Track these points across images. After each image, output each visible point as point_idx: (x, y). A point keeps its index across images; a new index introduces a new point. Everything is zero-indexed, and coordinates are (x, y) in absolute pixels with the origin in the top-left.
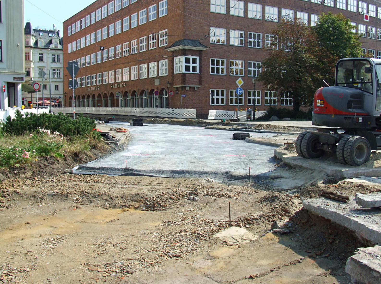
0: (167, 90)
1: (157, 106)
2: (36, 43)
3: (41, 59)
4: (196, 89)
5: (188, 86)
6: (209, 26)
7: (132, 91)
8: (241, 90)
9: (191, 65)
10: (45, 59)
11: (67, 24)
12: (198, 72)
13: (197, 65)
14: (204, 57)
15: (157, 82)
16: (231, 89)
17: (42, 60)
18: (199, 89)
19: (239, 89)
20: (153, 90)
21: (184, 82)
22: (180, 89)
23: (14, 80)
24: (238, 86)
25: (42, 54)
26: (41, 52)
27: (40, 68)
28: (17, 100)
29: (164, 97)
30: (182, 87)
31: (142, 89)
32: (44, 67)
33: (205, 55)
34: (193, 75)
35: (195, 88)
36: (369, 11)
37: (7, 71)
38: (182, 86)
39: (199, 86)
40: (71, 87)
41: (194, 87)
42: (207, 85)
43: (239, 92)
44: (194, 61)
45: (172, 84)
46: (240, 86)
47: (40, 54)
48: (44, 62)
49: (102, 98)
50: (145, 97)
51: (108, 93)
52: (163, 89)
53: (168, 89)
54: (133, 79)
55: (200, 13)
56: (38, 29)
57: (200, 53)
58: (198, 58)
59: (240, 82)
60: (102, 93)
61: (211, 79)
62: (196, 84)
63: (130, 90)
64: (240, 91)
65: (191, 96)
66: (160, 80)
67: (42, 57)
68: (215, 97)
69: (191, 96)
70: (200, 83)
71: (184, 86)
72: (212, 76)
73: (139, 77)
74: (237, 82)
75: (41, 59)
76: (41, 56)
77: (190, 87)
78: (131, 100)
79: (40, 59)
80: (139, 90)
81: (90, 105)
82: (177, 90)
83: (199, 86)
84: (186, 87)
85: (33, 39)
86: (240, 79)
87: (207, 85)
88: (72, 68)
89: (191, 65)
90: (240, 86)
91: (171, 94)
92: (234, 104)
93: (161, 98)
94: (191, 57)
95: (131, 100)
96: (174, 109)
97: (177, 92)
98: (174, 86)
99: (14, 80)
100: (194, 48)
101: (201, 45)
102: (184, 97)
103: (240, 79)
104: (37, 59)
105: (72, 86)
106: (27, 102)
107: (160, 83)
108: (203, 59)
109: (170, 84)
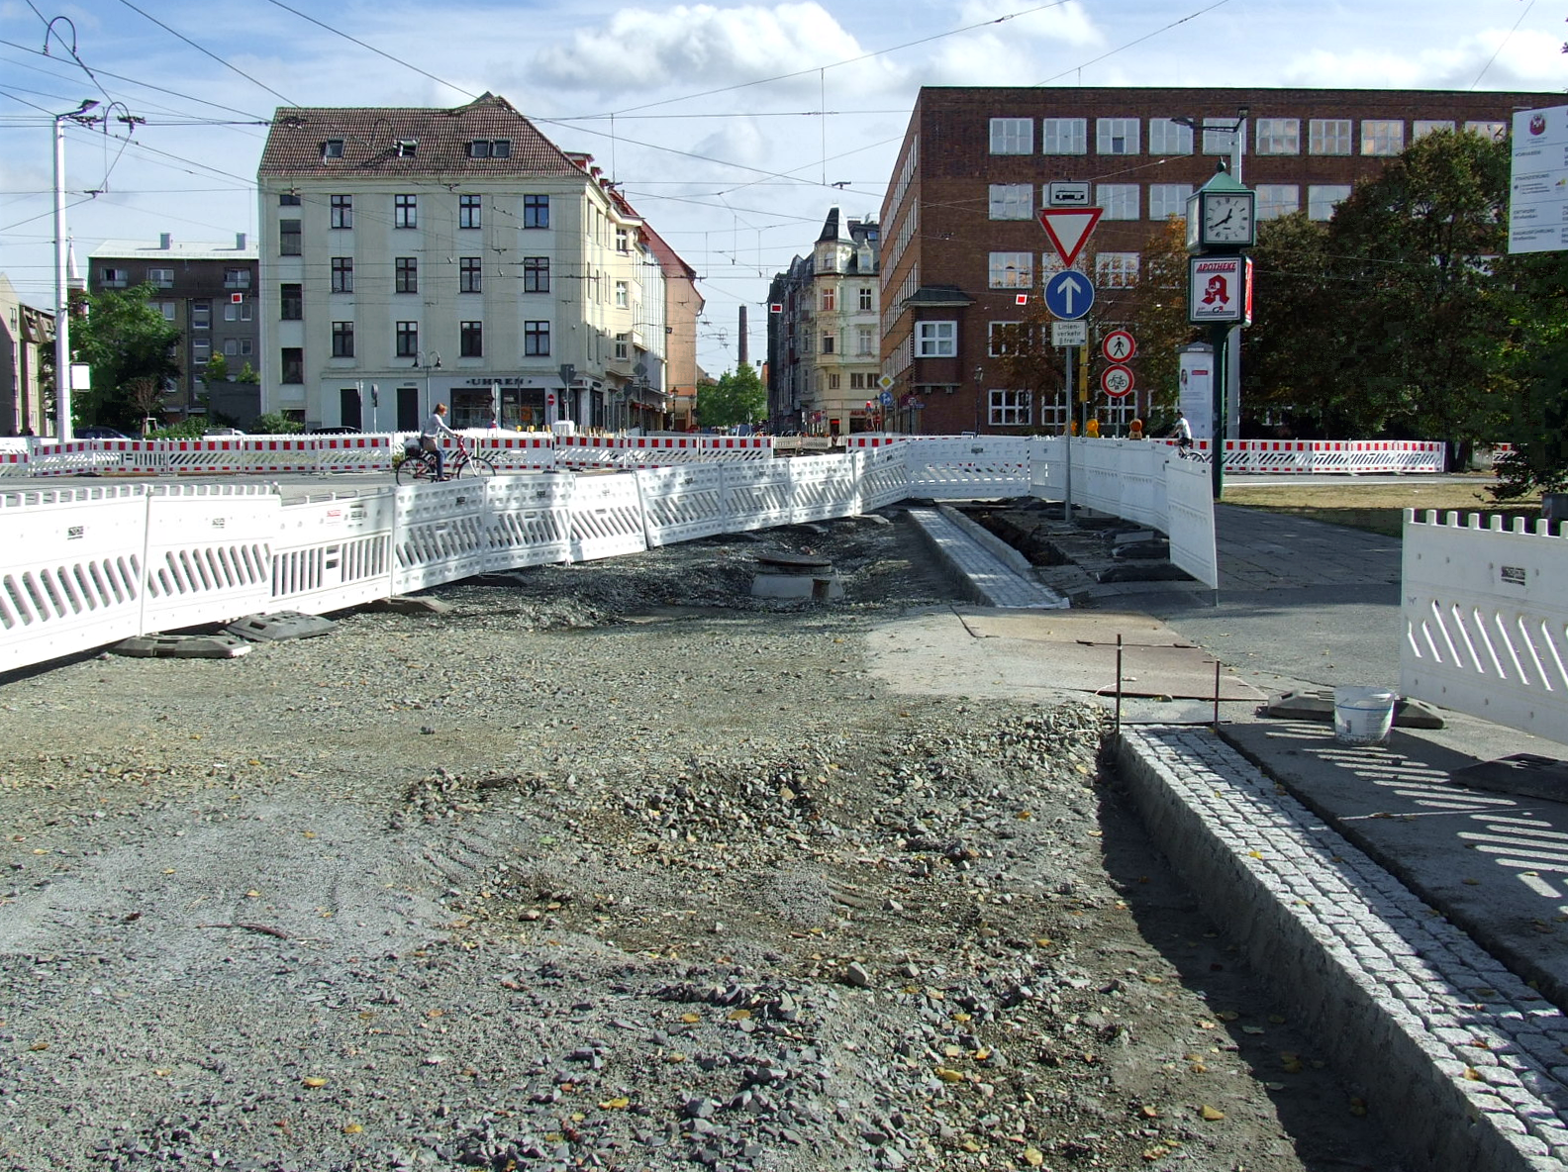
2: (853, 262)
4: (948, 390)
6: (986, 251)
12: (954, 354)
13: (954, 338)
17: (869, 307)
25: (869, 292)
26: (866, 287)
47: (862, 292)
48: (874, 313)
58: (954, 324)
62: (947, 380)
67: (869, 299)
68: (1004, 407)
76: (866, 296)
79: (862, 307)
85: (843, 251)
100: (939, 304)
101: (962, 296)
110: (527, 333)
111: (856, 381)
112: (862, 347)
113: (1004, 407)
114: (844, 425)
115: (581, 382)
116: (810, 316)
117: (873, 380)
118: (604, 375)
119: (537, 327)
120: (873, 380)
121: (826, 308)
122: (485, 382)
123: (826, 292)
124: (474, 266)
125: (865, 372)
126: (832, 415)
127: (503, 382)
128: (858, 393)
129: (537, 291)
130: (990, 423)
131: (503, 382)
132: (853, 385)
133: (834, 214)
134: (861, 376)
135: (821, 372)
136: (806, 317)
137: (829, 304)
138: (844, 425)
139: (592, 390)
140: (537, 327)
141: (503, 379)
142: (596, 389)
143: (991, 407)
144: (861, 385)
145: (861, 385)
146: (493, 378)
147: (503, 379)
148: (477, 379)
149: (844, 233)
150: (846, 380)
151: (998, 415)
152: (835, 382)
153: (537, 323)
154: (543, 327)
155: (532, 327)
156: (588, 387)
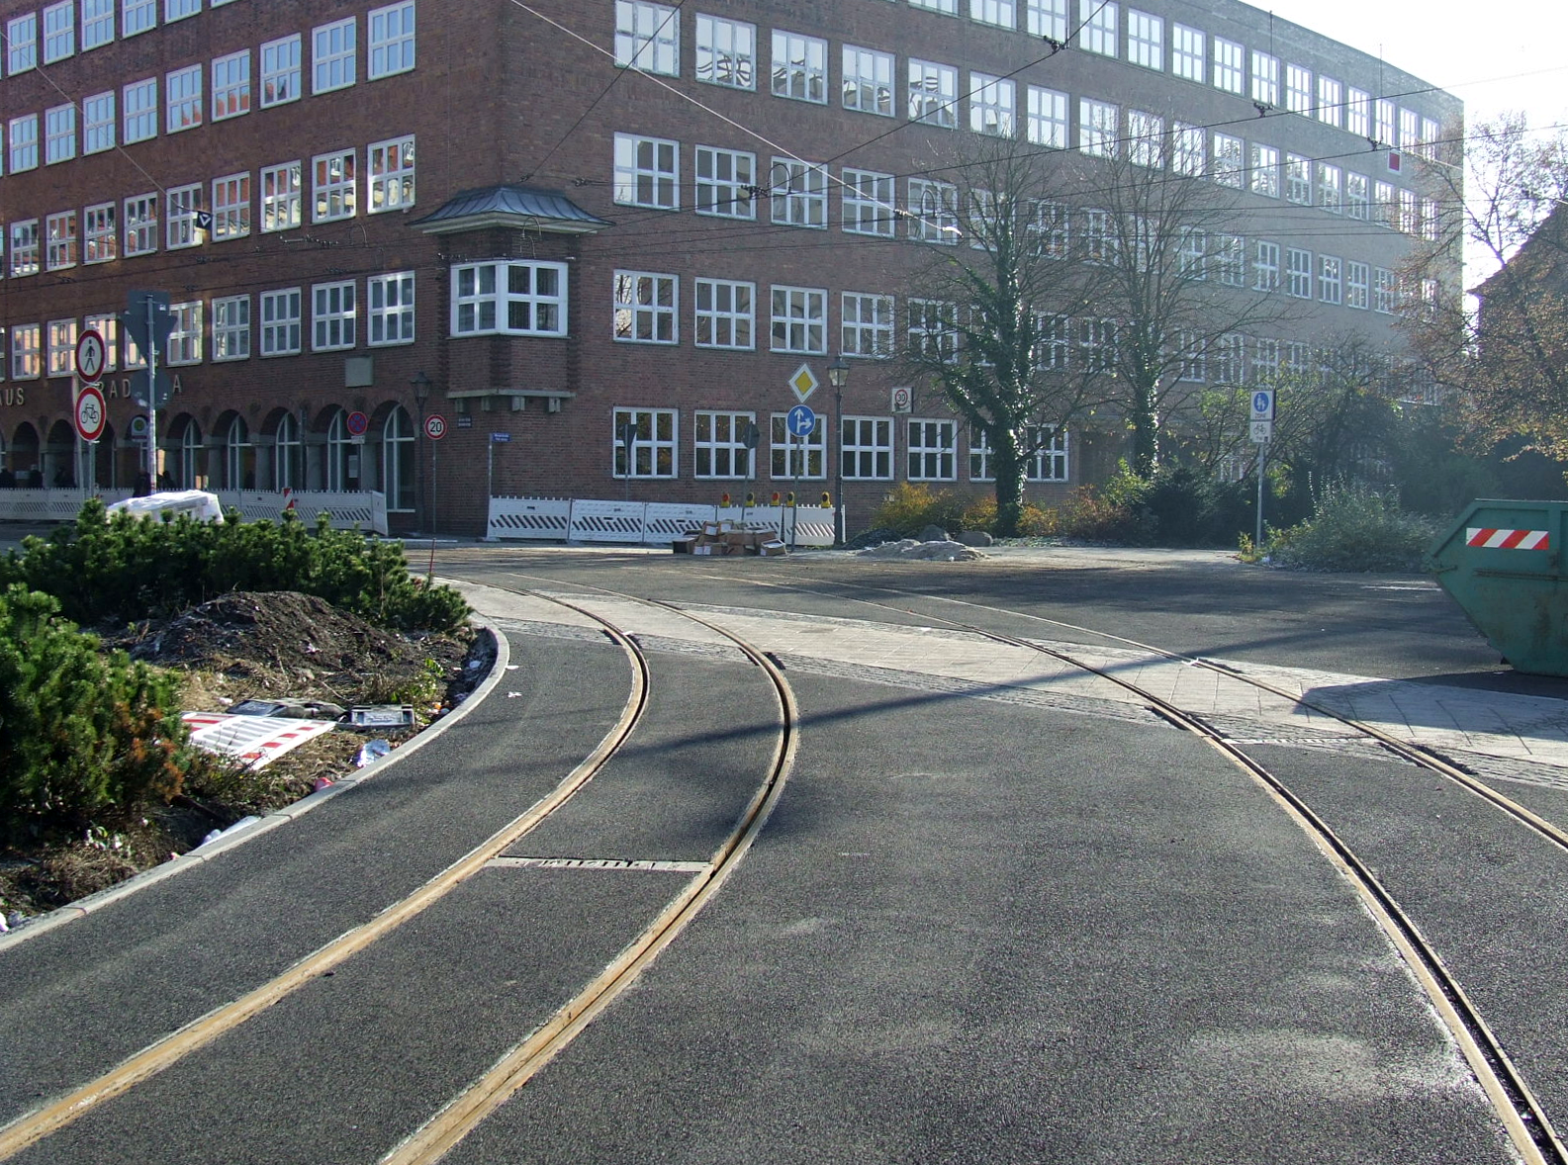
0: (413, 413)
1: (351, 485)
4: (553, 407)
5: (518, 394)
7: (216, 414)
8: (807, 414)
9: (533, 298)
12: (562, 330)
13: (560, 300)
15: (359, 374)
16: (703, 408)
18: (567, 406)
19: (799, 413)
20: (329, 411)
21: (499, 376)
22: (485, 406)
24: (798, 402)
29: (390, 444)
30: (493, 398)
31: (276, 403)
36: (1321, 104)
38: (494, 391)
39: (568, 394)
40: (142, 403)
41: (546, 399)
43: (799, 424)
44: (546, 282)
45: (439, 383)
46: (802, 398)
49: (43, 446)
50: (287, 443)
51: (43, 420)
52: (391, 404)
53: (421, 408)
54: (221, 354)
55: (570, 72)
57: (565, 245)
58: (562, 269)
59: (803, 383)
60: (43, 420)
63: (207, 410)
64: (803, 420)
65: (529, 437)
66: (374, 366)
69: (529, 437)
70: (572, 383)
71: (504, 392)
73: (256, 348)
74: (792, 382)
77: (529, 400)
78: (212, 455)
80: (255, 409)
81: (258, 481)
82: (466, 414)
83: (568, 394)
84: (510, 398)
86: (805, 368)
88: (147, 317)
89: (533, 298)
90: (802, 398)
91: (435, 427)
92: (713, 476)
93: (377, 447)
94: (534, 266)
95: (212, 455)
96: (537, 503)
97: (465, 422)
98: (451, 395)
102: (502, 443)
103: (805, 368)
105: (147, 398)
107: (375, 377)
109: (429, 383)
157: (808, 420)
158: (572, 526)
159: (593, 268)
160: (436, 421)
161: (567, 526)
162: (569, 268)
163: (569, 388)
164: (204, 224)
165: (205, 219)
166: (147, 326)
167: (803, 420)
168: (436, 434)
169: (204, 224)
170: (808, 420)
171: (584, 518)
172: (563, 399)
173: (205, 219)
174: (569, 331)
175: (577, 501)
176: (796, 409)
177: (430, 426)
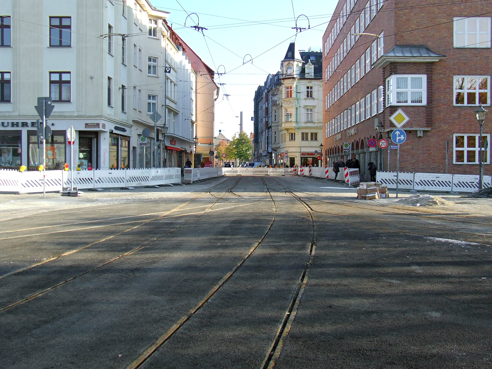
2: (303, 71)
3: (309, 95)
4: (419, 134)
10: (315, 95)
11: (325, 38)
12: (424, 103)
14: (440, 74)
17: (311, 96)
19: (398, 133)
23: (86, 128)
25: (311, 88)
26: (309, 85)
27: (308, 108)
28: (100, 156)
32: (314, 107)
33: (441, 72)
34: (412, 109)
35: (418, 132)
37: (76, 114)
39: (429, 129)
42: (445, 127)
43: (398, 138)
46: (399, 126)
47: (308, 88)
56: (315, 52)
58: (424, 77)
61: (456, 115)
62: (419, 126)
64: (399, 136)
65: (409, 147)
68: (466, 149)
69: (409, 147)
72: (458, 109)
75: (309, 95)
79: (308, 96)
83: (427, 129)
87: (445, 127)
88: (43, 107)
99: (86, 128)
103: (400, 111)
104: (303, 95)
106: (289, 158)
108: (435, 77)
110: (51, 82)
111: (304, 137)
112: (308, 118)
113: (466, 149)
114: (298, 162)
115: (98, 125)
116: (278, 103)
117: (314, 137)
118: (131, 123)
119: (60, 77)
120: (314, 137)
121: (288, 96)
122: (13, 125)
123: (288, 88)
124: (5, 24)
125: (309, 131)
126: (291, 155)
127: (30, 124)
128: (305, 143)
129: (61, 45)
130: (454, 162)
131: (30, 124)
132: (303, 139)
133: (292, 47)
134: (307, 134)
135: (285, 132)
136: (275, 104)
137: (289, 94)
138: (298, 162)
139: (111, 133)
140: (60, 77)
141: (29, 122)
142: (115, 131)
143: (455, 149)
144: (307, 139)
145: (307, 139)
146: (20, 121)
147: (29, 122)
148: (6, 121)
149: (297, 56)
150: (298, 137)
151: (460, 156)
152: (292, 137)
153: (60, 73)
154: (65, 77)
155: (56, 77)
156: (107, 129)
157: (402, 136)
158: (415, 184)
159: (442, 76)
160: (383, 141)
161: (412, 184)
162: (428, 77)
163: (427, 127)
164: (168, 71)
165: (168, 69)
166: (43, 110)
167: (399, 136)
168: (383, 146)
169: (168, 71)
170: (402, 136)
171: (421, 181)
172: (424, 131)
173: (168, 69)
174: (428, 103)
175: (455, 175)
176: (396, 131)
177: (381, 144)
